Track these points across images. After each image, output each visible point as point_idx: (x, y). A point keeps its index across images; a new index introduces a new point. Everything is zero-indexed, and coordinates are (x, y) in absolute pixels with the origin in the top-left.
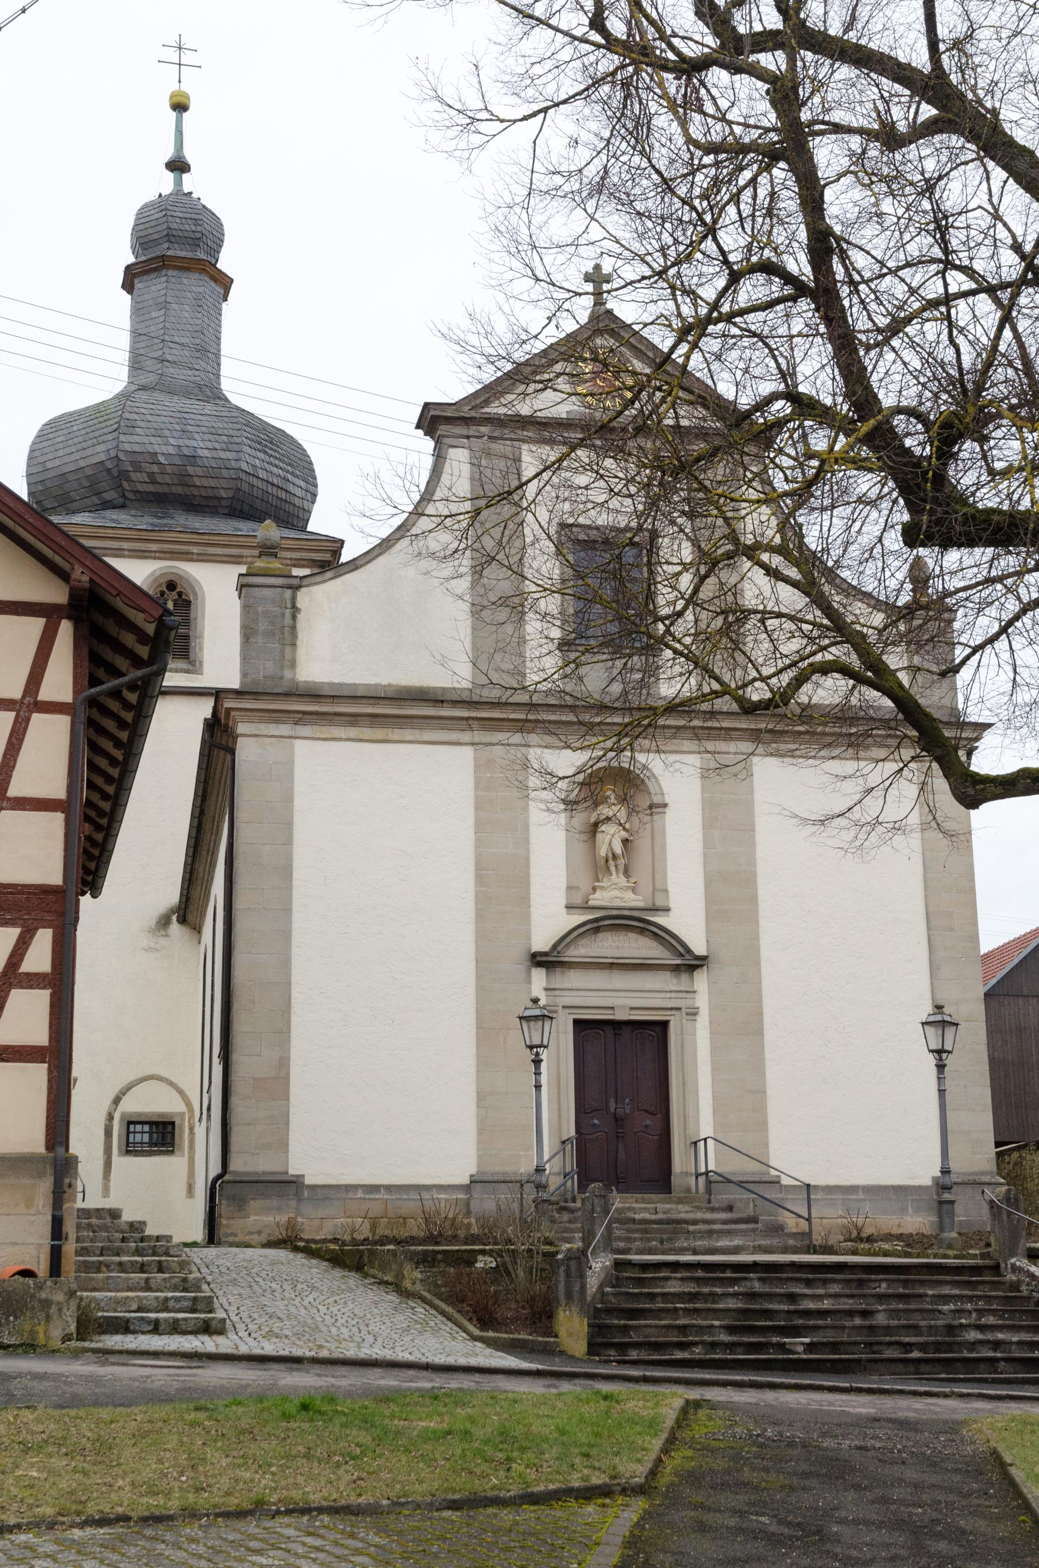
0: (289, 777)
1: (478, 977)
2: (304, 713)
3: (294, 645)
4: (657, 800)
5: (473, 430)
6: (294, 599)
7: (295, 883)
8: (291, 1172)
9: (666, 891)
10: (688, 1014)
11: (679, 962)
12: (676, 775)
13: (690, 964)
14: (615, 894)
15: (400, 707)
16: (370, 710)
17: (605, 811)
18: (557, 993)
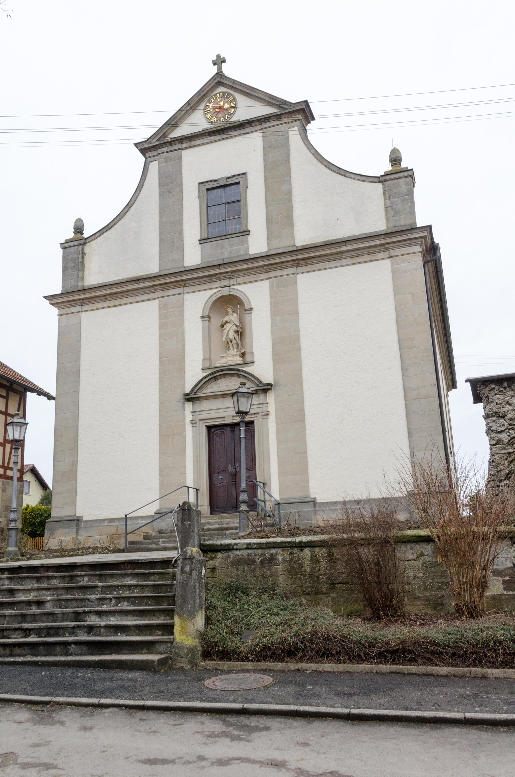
1: (160, 411)
2: (83, 299)
3: (83, 270)
4: (247, 307)
5: (160, 151)
6: (83, 250)
7: (81, 378)
8: (78, 515)
9: (252, 353)
10: (263, 415)
12: (257, 293)
14: (232, 358)
15: (121, 287)
16: (108, 292)
17: (226, 318)
18: (197, 413)
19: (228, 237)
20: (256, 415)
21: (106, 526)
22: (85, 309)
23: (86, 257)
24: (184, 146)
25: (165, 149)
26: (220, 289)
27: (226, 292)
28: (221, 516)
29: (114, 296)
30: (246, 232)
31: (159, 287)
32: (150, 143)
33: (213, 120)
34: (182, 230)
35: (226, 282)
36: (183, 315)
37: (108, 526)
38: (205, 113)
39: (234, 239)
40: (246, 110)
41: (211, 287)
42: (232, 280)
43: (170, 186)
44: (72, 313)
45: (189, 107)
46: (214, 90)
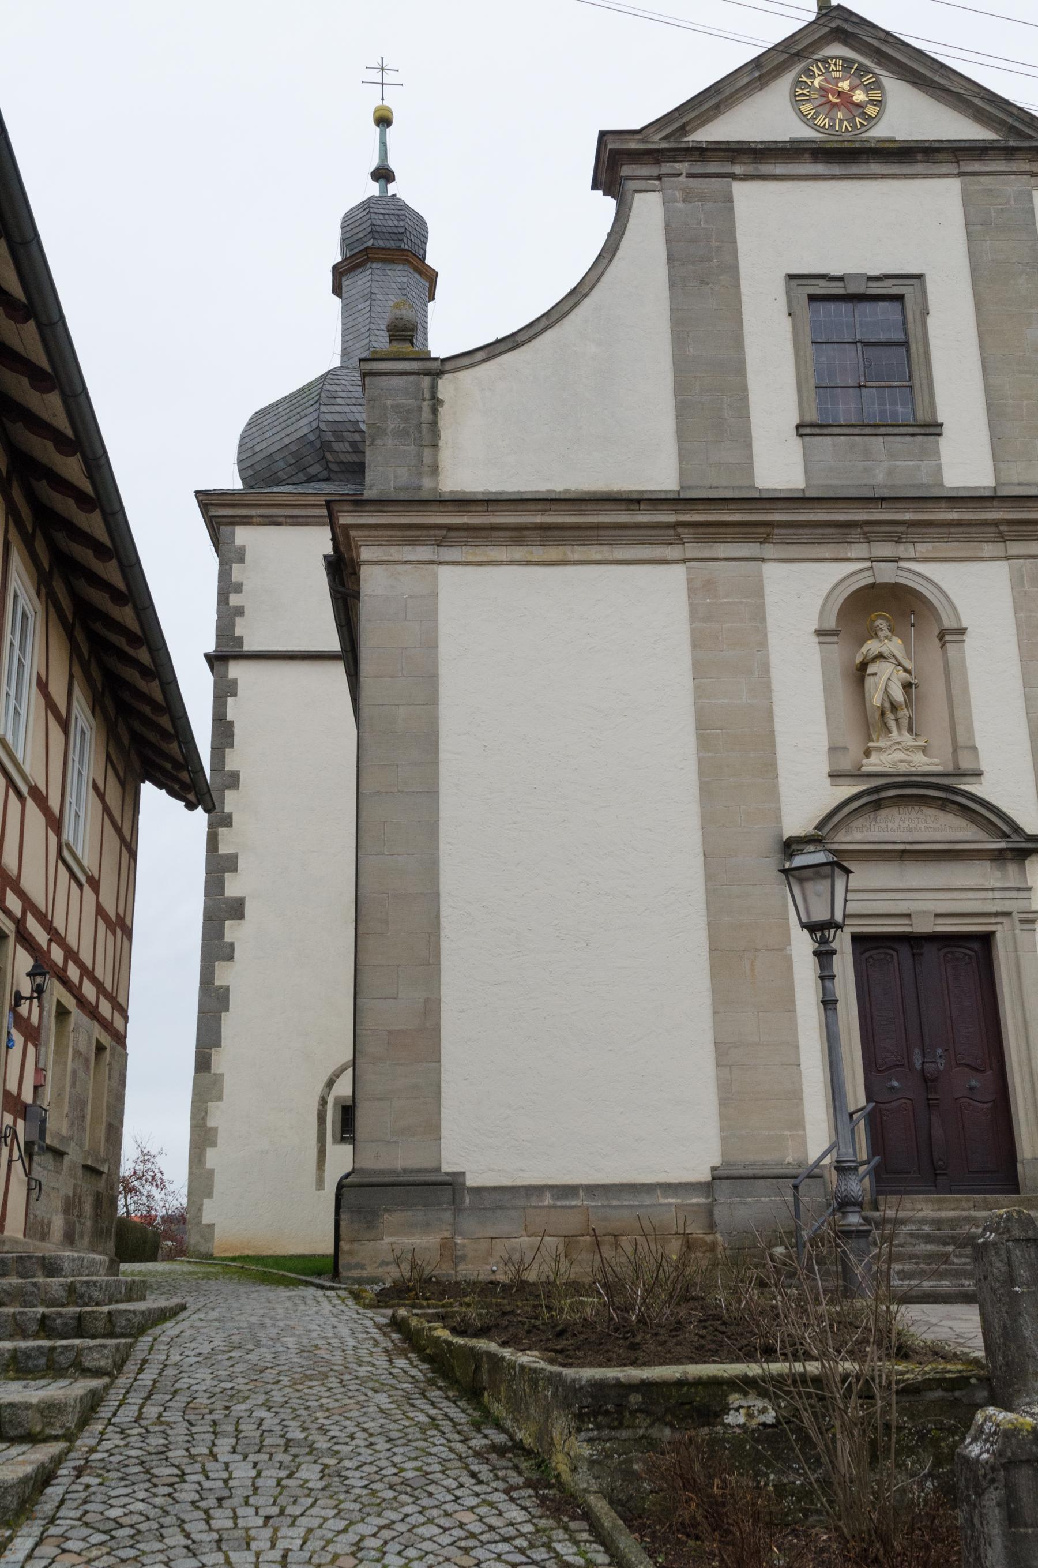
0: (431, 616)
1: (709, 877)
2: (449, 528)
3: (435, 446)
4: (948, 623)
5: (666, 168)
6: (434, 389)
7: (442, 756)
8: (446, 1168)
9: (974, 748)
10: (1022, 921)
11: (1003, 845)
13: (1020, 848)
14: (896, 755)
15: (581, 513)
16: (538, 519)
17: (872, 647)
19: (883, 430)
20: (999, 920)
21: (549, 1207)
22: (448, 558)
23: (442, 411)
24: (738, 169)
25: (683, 167)
26: (868, 564)
27: (887, 574)
28: (985, 1200)
29: (549, 533)
30: (933, 428)
31: (692, 531)
32: (644, 141)
33: (819, 121)
34: (744, 389)
35: (885, 550)
36: (764, 619)
37: (555, 1207)
38: (796, 100)
39: (898, 439)
40: (908, 115)
41: (842, 556)
42: (902, 547)
43: (702, 267)
44: (406, 562)
45: (757, 74)
46: (820, 48)
